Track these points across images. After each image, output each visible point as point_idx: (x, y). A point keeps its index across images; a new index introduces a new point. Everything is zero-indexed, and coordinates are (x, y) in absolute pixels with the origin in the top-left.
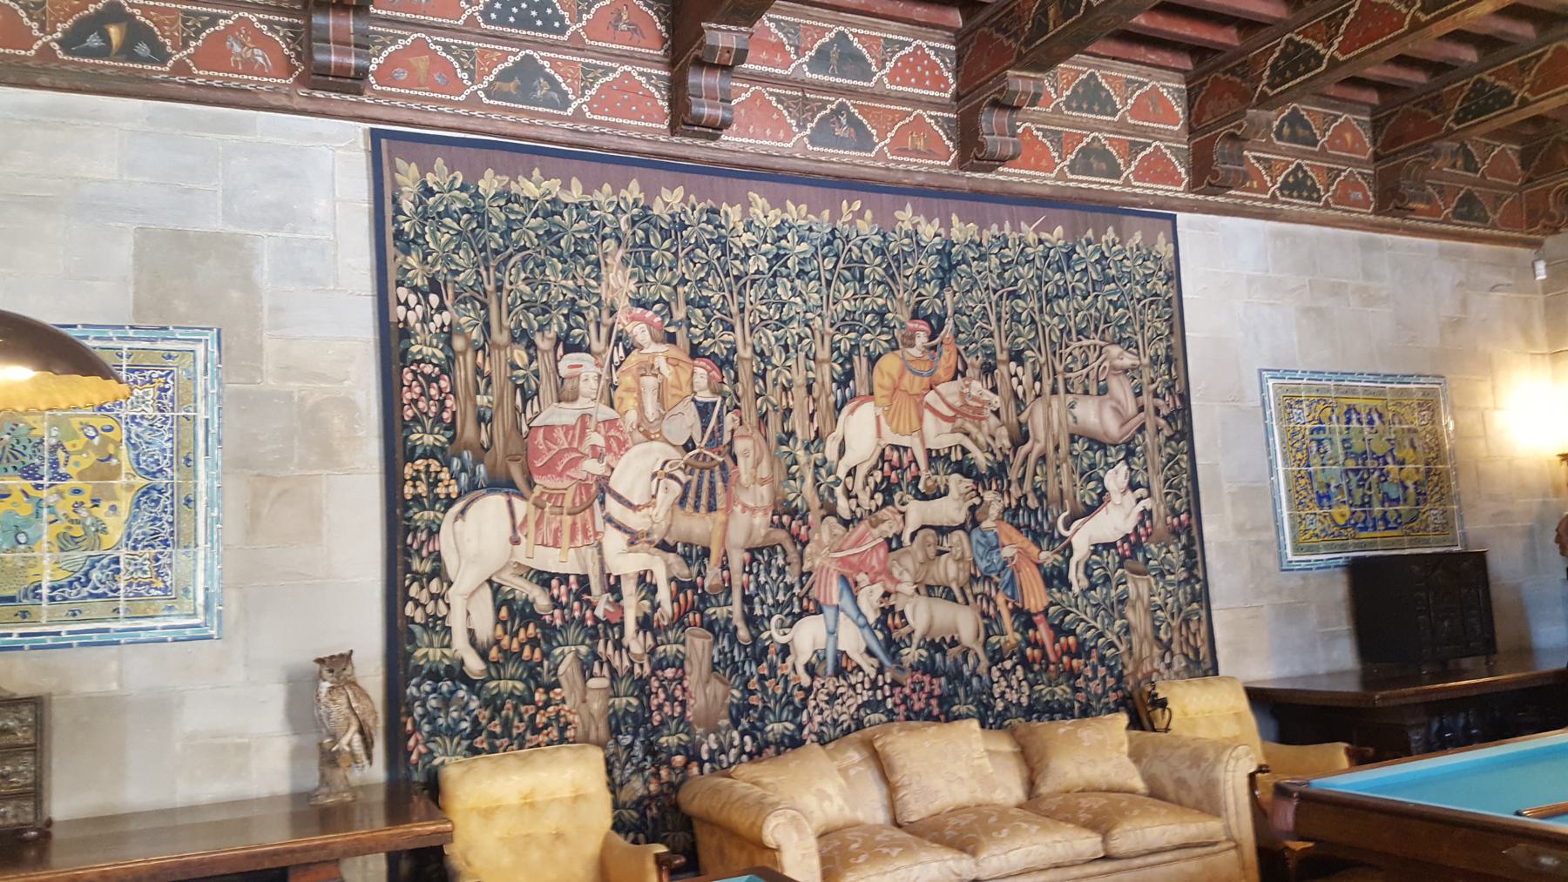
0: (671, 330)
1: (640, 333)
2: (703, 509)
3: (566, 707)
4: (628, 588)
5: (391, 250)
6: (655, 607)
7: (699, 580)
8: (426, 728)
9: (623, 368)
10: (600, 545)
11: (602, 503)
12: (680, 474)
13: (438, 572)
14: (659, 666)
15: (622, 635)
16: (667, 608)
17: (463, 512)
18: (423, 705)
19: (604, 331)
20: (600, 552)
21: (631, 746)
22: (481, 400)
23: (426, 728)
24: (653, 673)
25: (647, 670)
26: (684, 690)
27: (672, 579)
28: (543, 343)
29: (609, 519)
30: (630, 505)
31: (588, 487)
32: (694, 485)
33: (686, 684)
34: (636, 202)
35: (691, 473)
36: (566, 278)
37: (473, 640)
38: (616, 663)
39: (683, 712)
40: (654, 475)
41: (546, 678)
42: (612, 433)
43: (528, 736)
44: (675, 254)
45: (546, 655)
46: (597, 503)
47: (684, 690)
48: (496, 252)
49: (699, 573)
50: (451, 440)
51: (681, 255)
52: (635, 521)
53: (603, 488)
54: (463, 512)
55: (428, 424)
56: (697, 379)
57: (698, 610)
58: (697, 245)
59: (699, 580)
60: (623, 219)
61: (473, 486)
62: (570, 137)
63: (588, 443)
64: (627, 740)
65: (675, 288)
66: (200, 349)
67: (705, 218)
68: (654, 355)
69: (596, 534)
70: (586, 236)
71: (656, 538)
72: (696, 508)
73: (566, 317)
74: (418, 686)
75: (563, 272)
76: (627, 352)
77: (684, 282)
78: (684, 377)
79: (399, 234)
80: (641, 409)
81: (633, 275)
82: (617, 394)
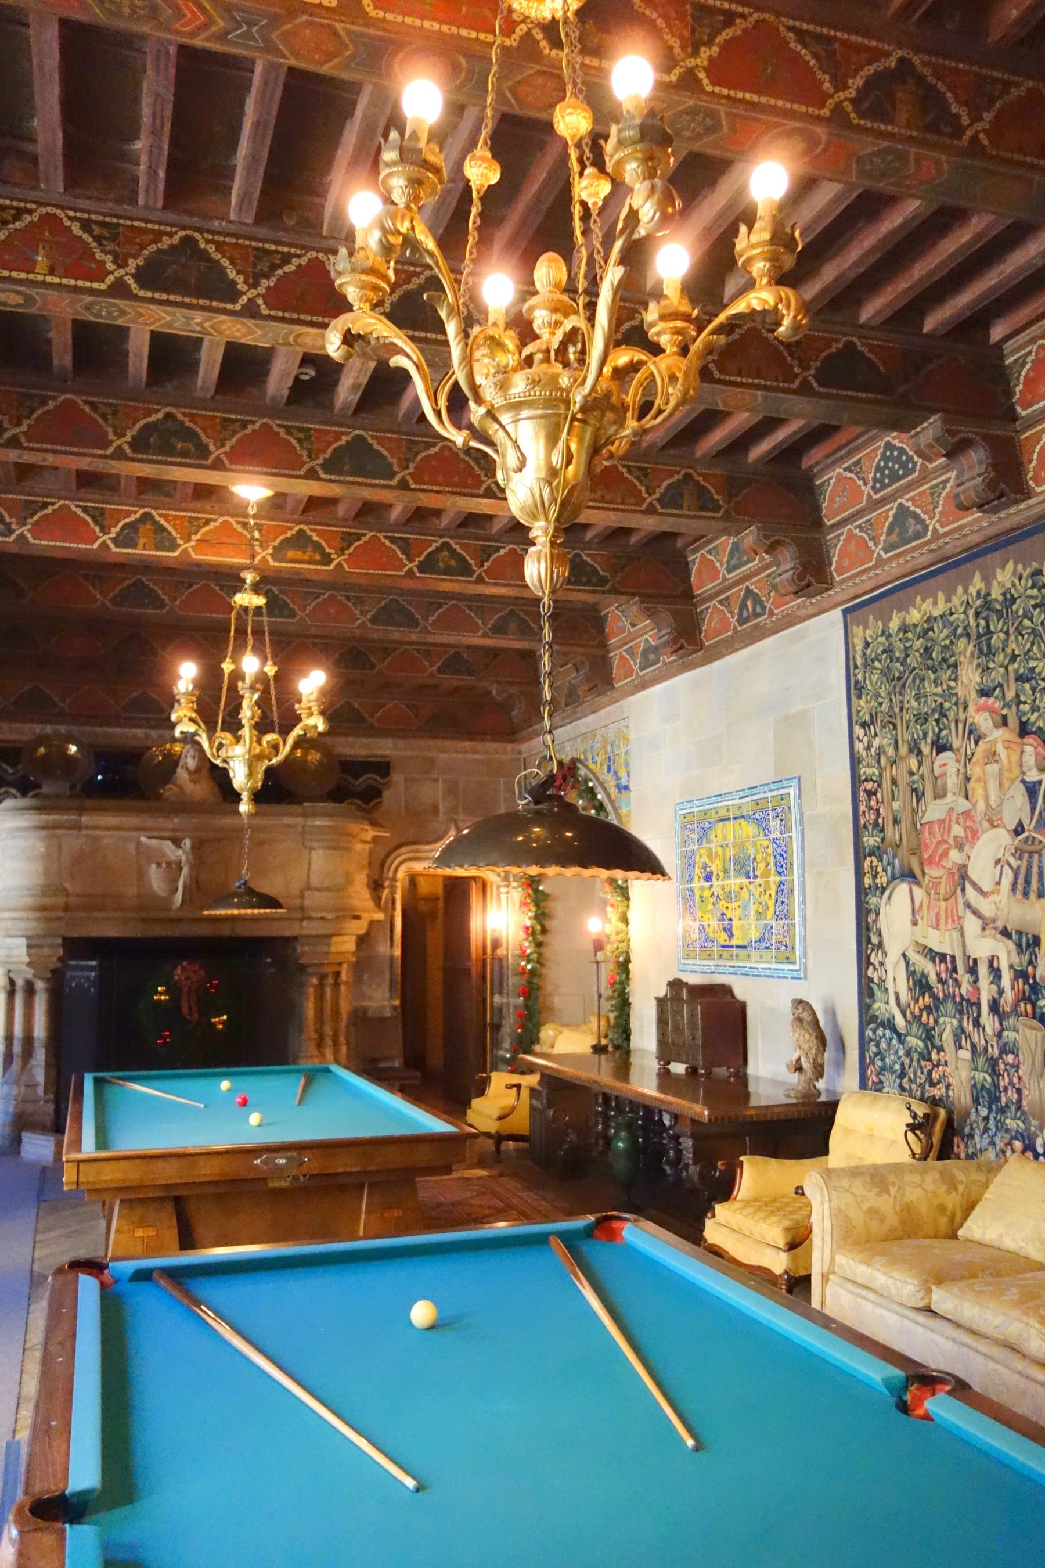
0: (1004, 712)
1: (983, 721)
2: (1033, 895)
3: (948, 1070)
4: (983, 970)
5: (854, 698)
6: (1001, 992)
7: (1030, 969)
8: (879, 1063)
9: (974, 760)
10: (962, 929)
11: (963, 890)
12: (1012, 860)
13: (880, 945)
14: (1004, 1051)
15: (979, 1015)
16: (1009, 996)
17: (889, 898)
18: (877, 1046)
19: (961, 726)
20: (962, 935)
21: (986, 1119)
22: (896, 805)
23: (879, 1063)
24: (1000, 1057)
25: (996, 1053)
26: (1020, 1078)
27: (1011, 967)
28: (926, 749)
29: (968, 905)
30: (981, 892)
31: (953, 874)
32: (1023, 870)
33: (1021, 1073)
34: (978, 593)
35: (1020, 858)
36: (936, 686)
37: (898, 1004)
38: (976, 1040)
39: (1020, 1100)
40: (998, 862)
41: (937, 1042)
42: (969, 823)
43: (927, 1087)
44: (1007, 633)
45: (936, 1021)
46: (959, 890)
47: (1020, 1078)
48: (899, 679)
49: (1030, 963)
50: (883, 840)
51: (1011, 631)
52: (986, 907)
53: (962, 877)
54: (889, 898)
55: (870, 828)
56: (1025, 758)
57: (1029, 1000)
58: (1025, 616)
59: (1030, 969)
60: (971, 613)
61: (894, 878)
62: (931, 557)
63: (952, 834)
64: (984, 1112)
65: (1006, 668)
66: (791, 791)
67: (1030, 584)
68: (995, 742)
69: (959, 918)
70: (947, 642)
71: (1000, 924)
72: (1026, 894)
73: (937, 721)
74: (874, 1031)
75: (935, 681)
76: (977, 743)
77: (1014, 658)
78: (1015, 757)
79: (857, 682)
80: (987, 798)
81: (978, 666)
82: (972, 784)
